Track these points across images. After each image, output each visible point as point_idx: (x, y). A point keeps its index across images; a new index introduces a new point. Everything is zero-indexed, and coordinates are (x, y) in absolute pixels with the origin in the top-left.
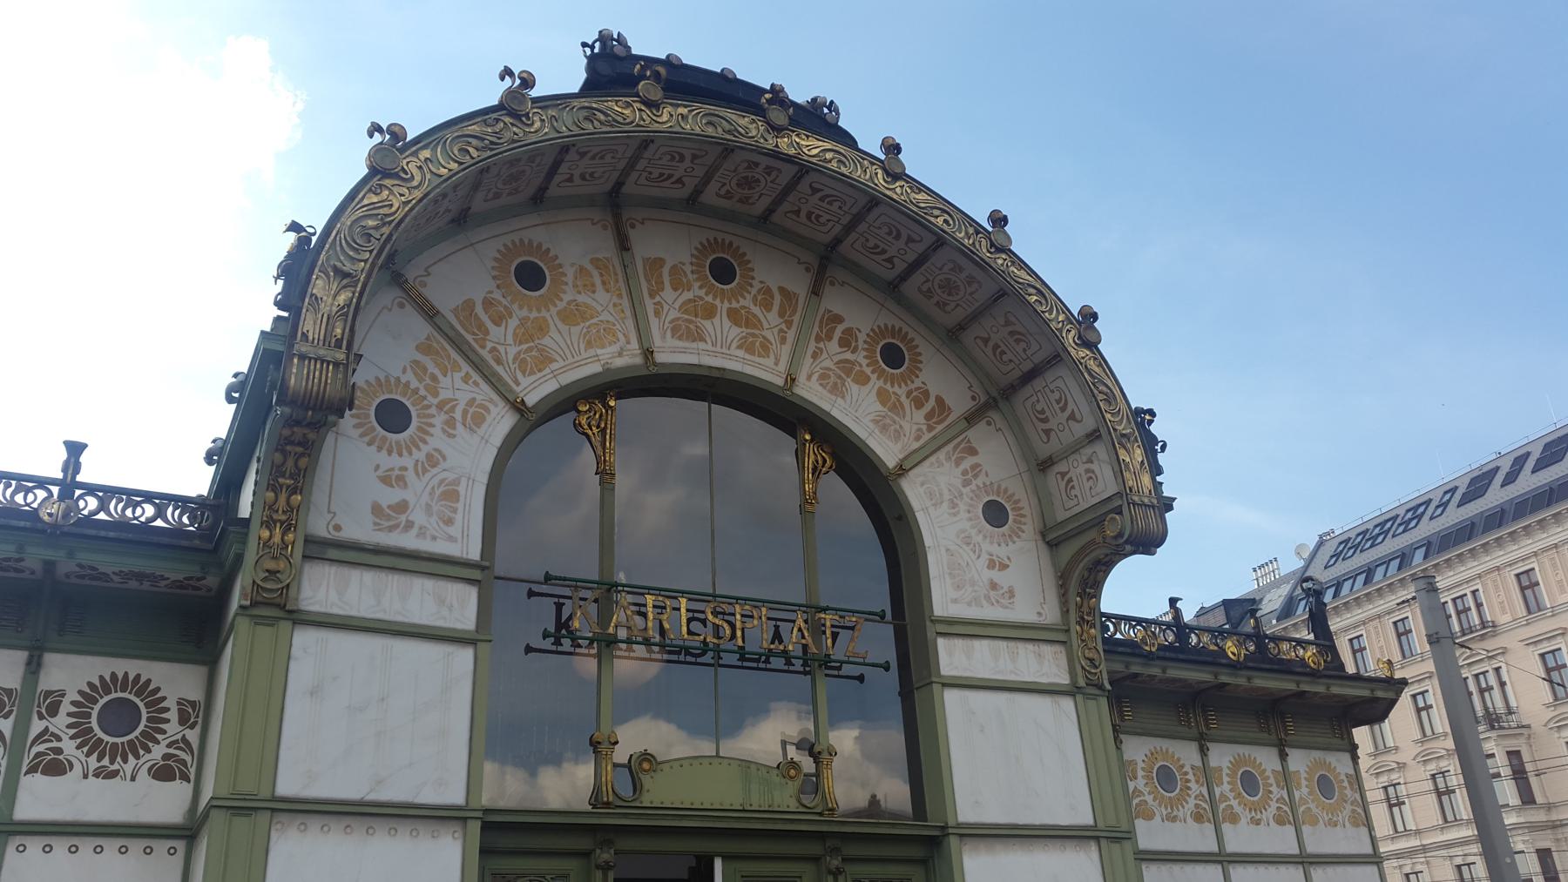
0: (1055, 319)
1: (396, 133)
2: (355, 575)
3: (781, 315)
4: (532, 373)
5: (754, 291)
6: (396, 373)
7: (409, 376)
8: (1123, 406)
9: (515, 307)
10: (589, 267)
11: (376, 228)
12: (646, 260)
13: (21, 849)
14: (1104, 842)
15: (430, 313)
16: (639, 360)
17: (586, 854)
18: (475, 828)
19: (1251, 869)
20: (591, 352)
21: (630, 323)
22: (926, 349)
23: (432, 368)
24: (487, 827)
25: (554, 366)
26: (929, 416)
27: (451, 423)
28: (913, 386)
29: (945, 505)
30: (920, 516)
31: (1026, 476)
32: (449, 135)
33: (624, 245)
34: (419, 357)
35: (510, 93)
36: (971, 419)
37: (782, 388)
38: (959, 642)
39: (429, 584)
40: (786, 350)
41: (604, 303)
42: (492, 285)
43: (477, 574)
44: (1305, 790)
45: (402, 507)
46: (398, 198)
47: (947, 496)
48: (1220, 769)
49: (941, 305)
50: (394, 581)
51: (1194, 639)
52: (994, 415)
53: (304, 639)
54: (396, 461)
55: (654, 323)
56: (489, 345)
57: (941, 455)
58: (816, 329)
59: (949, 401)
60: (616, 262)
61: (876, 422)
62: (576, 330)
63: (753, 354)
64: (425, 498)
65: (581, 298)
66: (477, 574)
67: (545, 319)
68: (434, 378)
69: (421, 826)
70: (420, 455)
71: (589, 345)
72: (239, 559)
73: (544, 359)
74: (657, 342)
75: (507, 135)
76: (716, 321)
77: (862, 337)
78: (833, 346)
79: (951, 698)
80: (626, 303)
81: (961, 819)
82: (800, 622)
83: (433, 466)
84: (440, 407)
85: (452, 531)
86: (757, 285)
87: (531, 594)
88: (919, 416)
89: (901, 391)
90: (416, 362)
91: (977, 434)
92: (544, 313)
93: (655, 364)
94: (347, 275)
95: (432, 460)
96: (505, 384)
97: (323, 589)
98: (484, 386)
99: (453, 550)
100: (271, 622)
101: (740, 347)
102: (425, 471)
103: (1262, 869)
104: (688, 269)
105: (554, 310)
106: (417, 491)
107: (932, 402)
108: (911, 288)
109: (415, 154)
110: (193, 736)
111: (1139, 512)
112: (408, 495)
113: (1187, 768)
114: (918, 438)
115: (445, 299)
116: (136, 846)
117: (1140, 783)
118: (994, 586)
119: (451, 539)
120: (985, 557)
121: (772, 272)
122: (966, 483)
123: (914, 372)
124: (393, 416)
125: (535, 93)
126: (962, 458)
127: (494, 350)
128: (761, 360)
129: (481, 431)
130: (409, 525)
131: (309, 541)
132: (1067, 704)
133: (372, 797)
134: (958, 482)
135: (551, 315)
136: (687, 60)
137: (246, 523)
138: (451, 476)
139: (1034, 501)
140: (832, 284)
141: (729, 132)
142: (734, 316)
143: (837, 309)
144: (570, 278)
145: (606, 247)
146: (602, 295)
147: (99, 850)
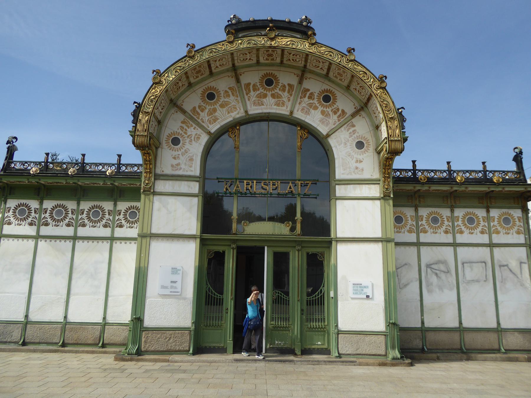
2: (167, 182)
3: (288, 92)
4: (213, 123)
5: (279, 87)
6: (176, 130)
7: (180, 131)
8: (393, 108)
9: (207, 106)
10: (228, 90)
11: (154, 98)
13: (116, 243)
15: (184, 112)
16: (244, 114)
18: (198, 240)
19: (466, 248)
20: (229, 115)
21: (241, 104)
23: (185, 127)
25: (219, 121)
28: (333, 108)
29: (343, 144)
30: (334, 149)
31: (372, 132)
32: (172, 68)
33: (238, 81)
35: (189, 52)
37: (288, 115)
38: (343, 186)
39: (186, 183)
40: (290, 103)
41: (232, 99)
42: (200, 101)
43: (198, 179)
45: (178, 164)
47: (343, 141)
48: (459, 217)
49: (341, 80)
50: (177, 183)
51: (455, 174)
52: (362, 113)
53: (156, 198)
54: (177, 153)
55: (248, 102)
56: (200, 118)
57: (342, 128)
58: (300, 95)
61: (320, 121)
62: (225, 109)
63: (279, 106)
64: (185, 161)
66: (198, 179)
67: (215, 108)
68: (186, 130)
70: (183, 150)
71: (229, 113)
73: (215, 120)
74: (249, 108)
76: (267, 98)
77: (316, 95)
78: (306, 99)
80: (239, 98)
82: (291, 184)
83: (187, 153)
85: (191, 169)
86: (280, 84)
87: (219, 182)
88: (335, 117)
89: (329, 110)
90: (181, 126)
92: (215, 106)
93: (248, 114)
94: (148, 112)
95: (186, 152)
96: (205, 128)
97: (161, 186)
98: (199, 129)
101: (275, 105)
102: (184, 154)
103: (471, 248)
104: (258, 84)
106: (182, 160)
107: (340, 112)
108: (331, 74)
109: (164, 76)
112: (180, 161)
113: (444, 217)
114: (334, 124)
115: (188, 107)
117: (424, 222)
118: (357, 168)
119: (192, 171)
120: (355, 159)
121: (286, 78)
122: (351, 136)
123: (334, 103)
124: (176, 141)
125: (195, 49)
126: (349, 129)
127: (202, 119)
128: (282, 108)
129: (199, 142)
130: (181, 169)
132: (378, 203)
133: (173, 233)
134: (348, 137)
135: (217, 106)
138: (191, 155)
139: (374, 139)
140: (306, 79)
141: (255, 44)
142: (273, 96)
143: (307, 87)
144: (222, 95)
145: (232, 82)
146: (232, 98)
147: (130, 243)
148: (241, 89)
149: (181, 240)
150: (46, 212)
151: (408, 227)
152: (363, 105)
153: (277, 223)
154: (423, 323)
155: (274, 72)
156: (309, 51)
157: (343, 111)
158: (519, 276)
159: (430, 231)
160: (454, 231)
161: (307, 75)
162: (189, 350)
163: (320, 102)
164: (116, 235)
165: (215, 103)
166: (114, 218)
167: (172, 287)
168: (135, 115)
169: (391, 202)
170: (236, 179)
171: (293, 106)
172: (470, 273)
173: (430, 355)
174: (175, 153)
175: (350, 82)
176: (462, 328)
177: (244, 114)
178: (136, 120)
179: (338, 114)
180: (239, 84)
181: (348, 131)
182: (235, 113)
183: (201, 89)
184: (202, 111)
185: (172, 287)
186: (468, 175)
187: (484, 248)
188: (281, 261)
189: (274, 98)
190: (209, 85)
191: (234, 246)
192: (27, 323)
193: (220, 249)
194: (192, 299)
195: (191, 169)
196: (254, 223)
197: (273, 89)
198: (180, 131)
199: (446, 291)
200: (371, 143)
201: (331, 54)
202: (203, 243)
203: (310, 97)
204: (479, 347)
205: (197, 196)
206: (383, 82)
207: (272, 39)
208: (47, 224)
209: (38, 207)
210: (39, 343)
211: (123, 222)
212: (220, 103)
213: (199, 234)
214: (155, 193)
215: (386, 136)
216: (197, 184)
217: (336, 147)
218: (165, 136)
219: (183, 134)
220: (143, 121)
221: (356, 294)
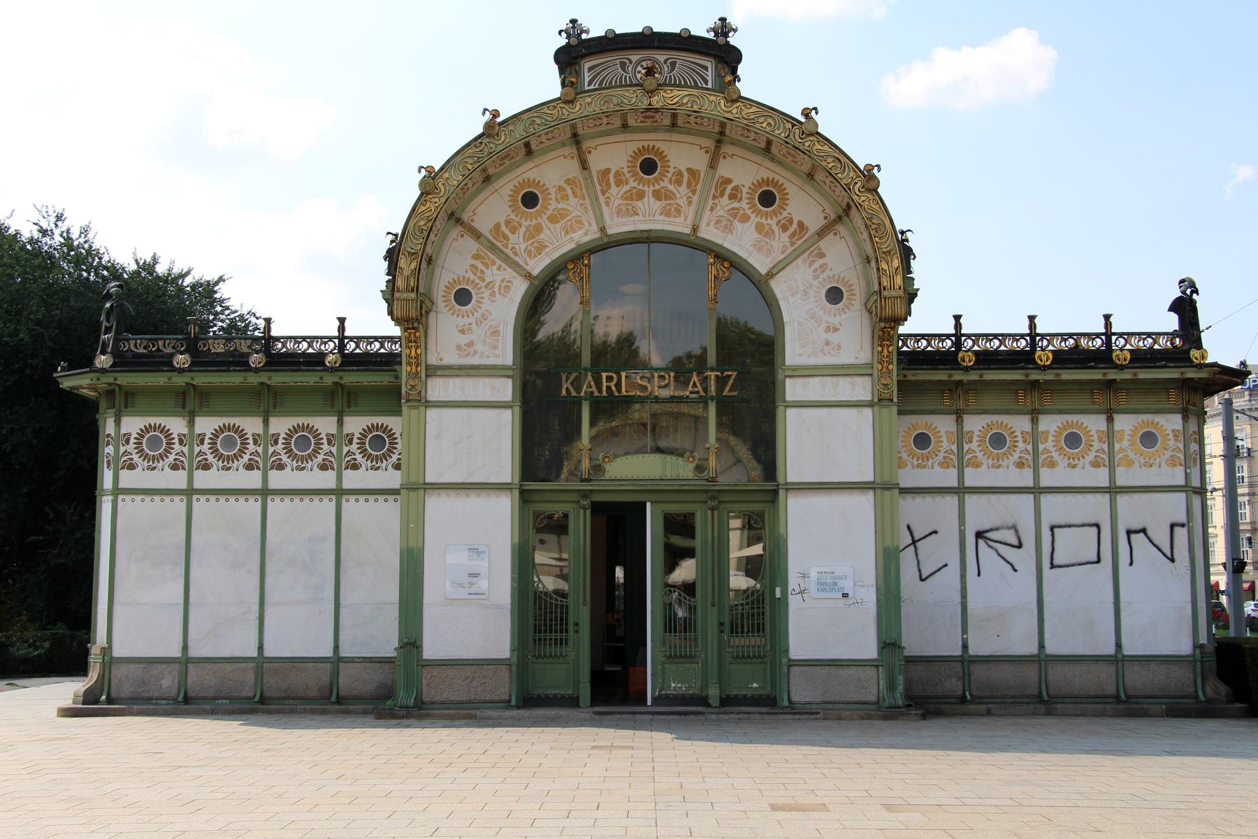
1: (429, 169)
2: (451, 381)
3: (689, 186)
5: (670, 175)
6: (462, 273)
7: (470, 275)
10: (565, 186)
12: (598, 172)
14: (878, 491)
15: (477, 235)
18: (516, 492)
19: (1060, 497)
20: (569, 237)
21: (591, 214)
23: (481, 267)
27: (493, 294)
28: (780, 217)
33: (584, 165)
34: (474, 262)
38: (800, 380)
39: (487, 380)
40: (692, 209)
41: (572, 204)
42: (509, 211)
44: (1125, 443)
48: (1048, 432)
52: (839, 227)
53: (431, 413)
54: (466, 321)
55: (605, 209)
57: (800, 261)
58: (713, 191)
60: (580, 178)
62: (558, 226)
66: (511, 373)
68: (482, 272)
69: (491, 492)
71: (567, 233)
73: (541, 248)
74: (608, 222)
76: (645, 200)
77: (745, 190)
78: (725, 200)
79: (791, 413)
80: (587, 201)
81: (789, 480)
84: (487, 286)
85: (496, 352)
86: (672, 170)
88: (785, 237)
89: (772, 222)
91: (826, 243)
96: (520, 266)
97: (438, 389)
100: (417, 408)
103: (1070, 497)
104: (626, 171)
105: (545, 217)
106: (478, 334)
107: (795, 225)
114: (783, 252)
115: (483, 224)
118: (828, 343)
119: (497, 356)
120: (824, 325)
121: (683, 155)
122: (816, 277)
124: (463, 297)
125: (499, 120)
130: (475, 352)
132: (868, 412)
135: (543, 221)
139: (863, 283)
142: (657, 195)
144: (553, 196)
147: (376, 500)
149: (484, 493)
151: (941, 455)
154: (965, 646)
155: (657, 144)
156: (727, 115)
157: (801, 224)
159: (986, 462)
161: (727, 149)
162: (510, 701)
163: (753, 206)
165: (540, 214)
166: (340, 450)
168: (392, 256)
169: (895, 409)
170: (586, 370)
171: (698, 215)
173: (972, 707)
174: (462, 321)
176: (1043, 656)
177: (598, 235)
178: (392, 270)
179: (791, 230)
180: (586, 172)
181: (810, 265)
182: (581, 232)
183: (510, 186)
184: (513, 231)
187: (1099, 496)
189: (660, 199)
190: (526, 176)
191: (586, 503)
192: (185, 662)
194: (509, 607)
195: (496, 352)
197: (657, 180)
198: (470, 275)
200: (857, 291)
201: (770, 121)
202: (526, 497)
203: (733, 197)
205: (511, 407)
206: (873, 178)
207: (651, 93)
209: (185, 431)
210: (216, 698)
212: (549, 213)
213: (517, 481)
214: (429, 404)
215: (876, 288)
216: (510, 382)
217: (786, 299)
218: (442, 288)
219: (477, 281)
220: (407, 272)
221: (824, 590)
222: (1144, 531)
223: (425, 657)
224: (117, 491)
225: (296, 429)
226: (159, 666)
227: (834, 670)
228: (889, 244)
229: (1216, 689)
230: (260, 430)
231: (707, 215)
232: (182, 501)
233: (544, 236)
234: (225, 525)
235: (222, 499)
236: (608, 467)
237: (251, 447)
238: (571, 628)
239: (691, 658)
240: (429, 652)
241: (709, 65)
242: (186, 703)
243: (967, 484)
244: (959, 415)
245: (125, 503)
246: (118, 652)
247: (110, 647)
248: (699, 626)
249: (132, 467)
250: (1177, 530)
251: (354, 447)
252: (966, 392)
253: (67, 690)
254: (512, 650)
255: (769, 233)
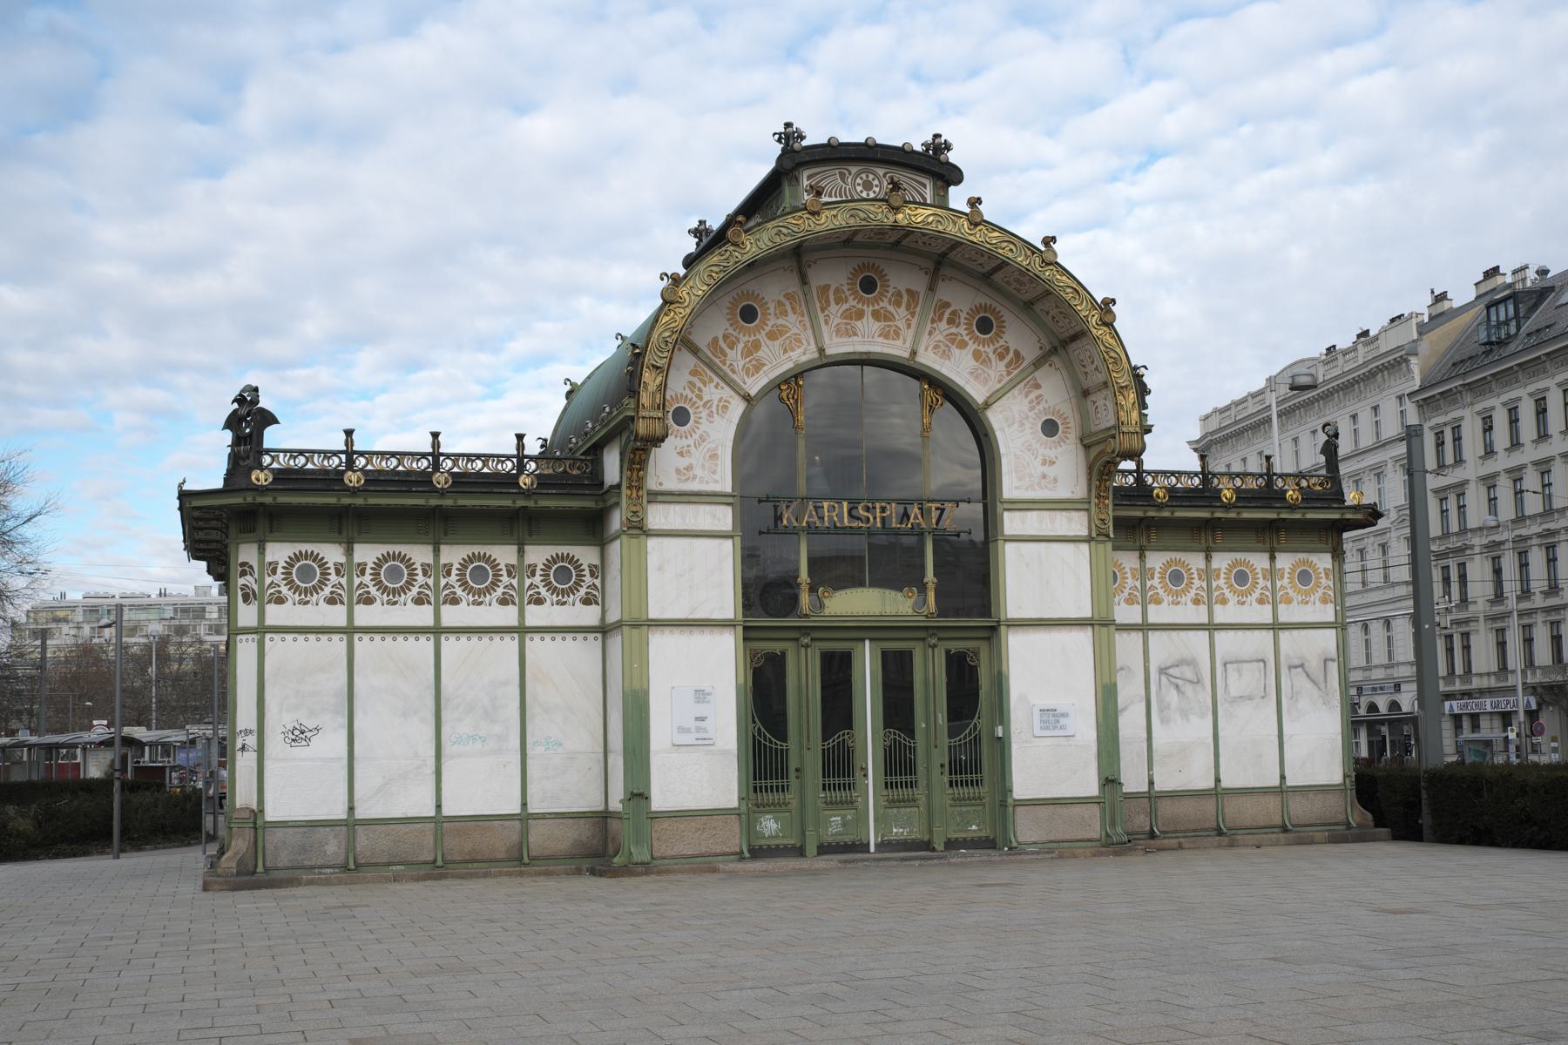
0: (1082, 309)
2: (672, 507)
6: (680, 391)
7: (687, 392)
16: (816, 355)
17: (797, 640)
18: (740, 629)
21: (810, 332)
22: (1008, 317)
23: (699, 384)
24: (745, 628)
26: (1008, 366)
27: (710, 415)
30: (998, 434)
33: (804, 281)
36: (1037, 364)
38: (1017, 514)
39: (707, 507)
43: (730, 500)
44: (1286, 581)
45: (689, 468)
46: (679, 315)
50: (690, 509)
52: (1055, 359)
53: (652, 543)
54: (685, 442)
55: (824, 328)
57: (1016, 391)
59: (1023, 353)
65: (780, 322)
66: (730, 500)
70: (696, 436)
71: (785, 351)
72: (617, 504)
73: (758, 367)
74: (827, 341)
75: (732, 261)
77: (963, 315)
78: (943, 325)
79: (1010, 548)
80: (806, 319)
86: (891, 290)
88: (1002, 366)
89: (989, 350)
97: (657, 517)
98: (727, 388)
99: (717, 488)
100: (637, 536)
103: (1240, 633)
104: (845, 288)
106: (697, 458)
107: (1011, 354)
110: (598, 582)
111: (1127, 437)
115: (702, 340)
116: (580, 636)
117: (1156, 582)
118: (1044, 476)
121: (901, 279)
122: (1032, 409)
124: (682, 417)
130: (695, 477)
131: (650, 493)
132: (1085, 547)
134: (1025, 409)
135: (762, 337)
136: (844, 138)
137: (619, 486)
139: (1077, 416)
142: (876, 316)
143: (946, 299)
144: (772, 310)
145: (793, 284)
146: (792, 317)
148: (809, 299)
149: (707, 630)
150: (363, 573)
151: (1127, 591)
152: (1056, 343)
153: (887, 592)
154: (1151, 783)
157: (1017, 354)
158: (1322, 686)
159: (1167, 599)
160: (1209, 599)
161: (946, 271)
164: (530, 621)
166: (521, 583)
167: (698, 729)
169: (1110, 545)
171: (916, 340)
172: (1237, 683)
175: (1038, 299)
185: (698, 729)
186: (1238, 482)
188: (896, 672)
192: (351, 824)
193: (777, 647)
196: (842, 592)
198: (687, 392)
199: (1194, 719)
200: (1072, 425)
203: (951, 322)
204: (1248, 823)
206: (1110, 312)
207: (896, 210)
208: (369, 601)
209: (342, 560)
210: (389, 864)
211: (543, 591)
212: (767, 329)
213: (740, 617)
216: (729, 509)
217: (1002, 429)
220: (652, 387)
222: (1302, 666)
223: (653, 808)
224: (261, 630)
225: (471, 559)
226: (321, 829)
227: (1059, 809)
228: (1125, 379)
229: (1359, 816)
230: (430, 560)
231: (925, 339)
232: (341, 640)
233: (763, 353)
234: (394, 669)
235: (389, 638)
236: (826, 602)
237: (420, 579)
238: (792, 774)
239: (912, 802)
240: (658, 802)
241: (927, 182)
242: (438, 869)
243: (1151, 620)
244: (1142, 552)
245: (273, 644)
246: (271, 815)
247: (262, 811)
248: (921, 768)
249: (280, 601)
250: (1330, 664)
251: (537, 579)
252: (1148, 528)
253: (192, 858)
254: (741, 799)
255: (986, 361)
